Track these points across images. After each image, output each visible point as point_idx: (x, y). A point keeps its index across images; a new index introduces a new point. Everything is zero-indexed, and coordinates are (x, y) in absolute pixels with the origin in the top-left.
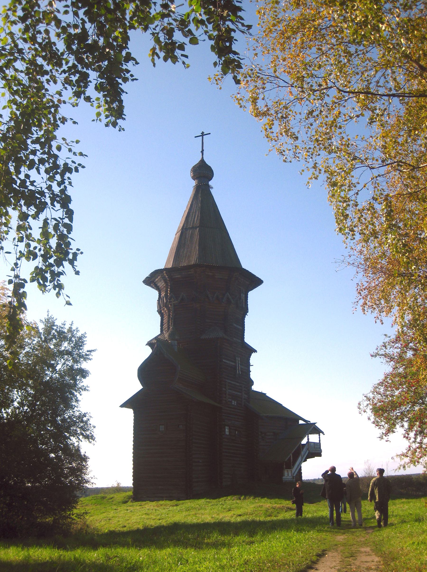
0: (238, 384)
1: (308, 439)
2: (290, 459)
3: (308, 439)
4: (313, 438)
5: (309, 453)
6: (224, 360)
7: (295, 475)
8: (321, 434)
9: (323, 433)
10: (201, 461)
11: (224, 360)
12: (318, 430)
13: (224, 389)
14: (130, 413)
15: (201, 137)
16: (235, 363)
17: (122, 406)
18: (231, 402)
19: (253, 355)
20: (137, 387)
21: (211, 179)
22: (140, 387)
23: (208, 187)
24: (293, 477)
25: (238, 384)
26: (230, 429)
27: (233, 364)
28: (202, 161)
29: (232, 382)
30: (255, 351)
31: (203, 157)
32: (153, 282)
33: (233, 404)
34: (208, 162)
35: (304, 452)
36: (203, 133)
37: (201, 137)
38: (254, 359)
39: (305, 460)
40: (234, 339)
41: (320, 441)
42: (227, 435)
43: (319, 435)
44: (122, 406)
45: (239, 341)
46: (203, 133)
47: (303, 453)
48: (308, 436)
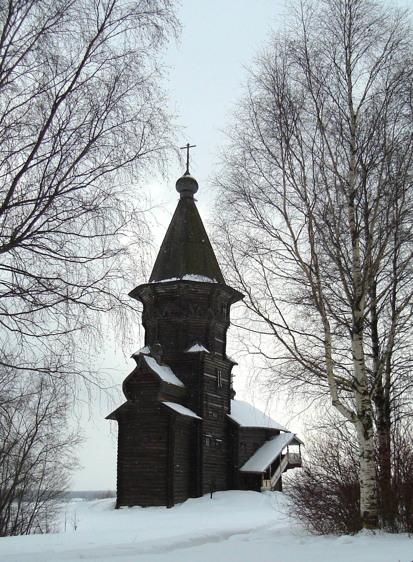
0: (218, 397)
1: (288, 450)
2: (268, 470)
3: (288, 450)
4: (294, 449)
5: (289, 463)
6: (205, 374)
7: (273, 486)
8: (301, 445)
9: (303, 444)
10: (181, 472)
11: (205, 374)
12: (297, 441)
13: (204, 402)
14: (114, 424)
15: (187, 149)
16: (217, 376)
17: (107, 418)
18: (212, 414)
19: (235, 367)
20: (121, 399)
21: (195, 193)
22: (124, 400)
23: (193, 199)
24: (272, 487)
25: (218, 397)
26: (210, 441)
27: (215, 377)
28: (187, 173)
29: (213, 395)
30: (237, 364)
31: (188, 169)
32: (138, 295)
33: (214, 416)
34: (193, 175)
35: (284, 463)
36: (188, 145)
37: (187, 149)
38: (235, 370)
39: (285, 471)
40: (216, 353)
41: (300, 451)
42: (207, 447)
43: (300, 446)
44: (107, 418)
45: (221, 355)
46: (188, 145)
47: (282, 464)
48: (288, 447)
